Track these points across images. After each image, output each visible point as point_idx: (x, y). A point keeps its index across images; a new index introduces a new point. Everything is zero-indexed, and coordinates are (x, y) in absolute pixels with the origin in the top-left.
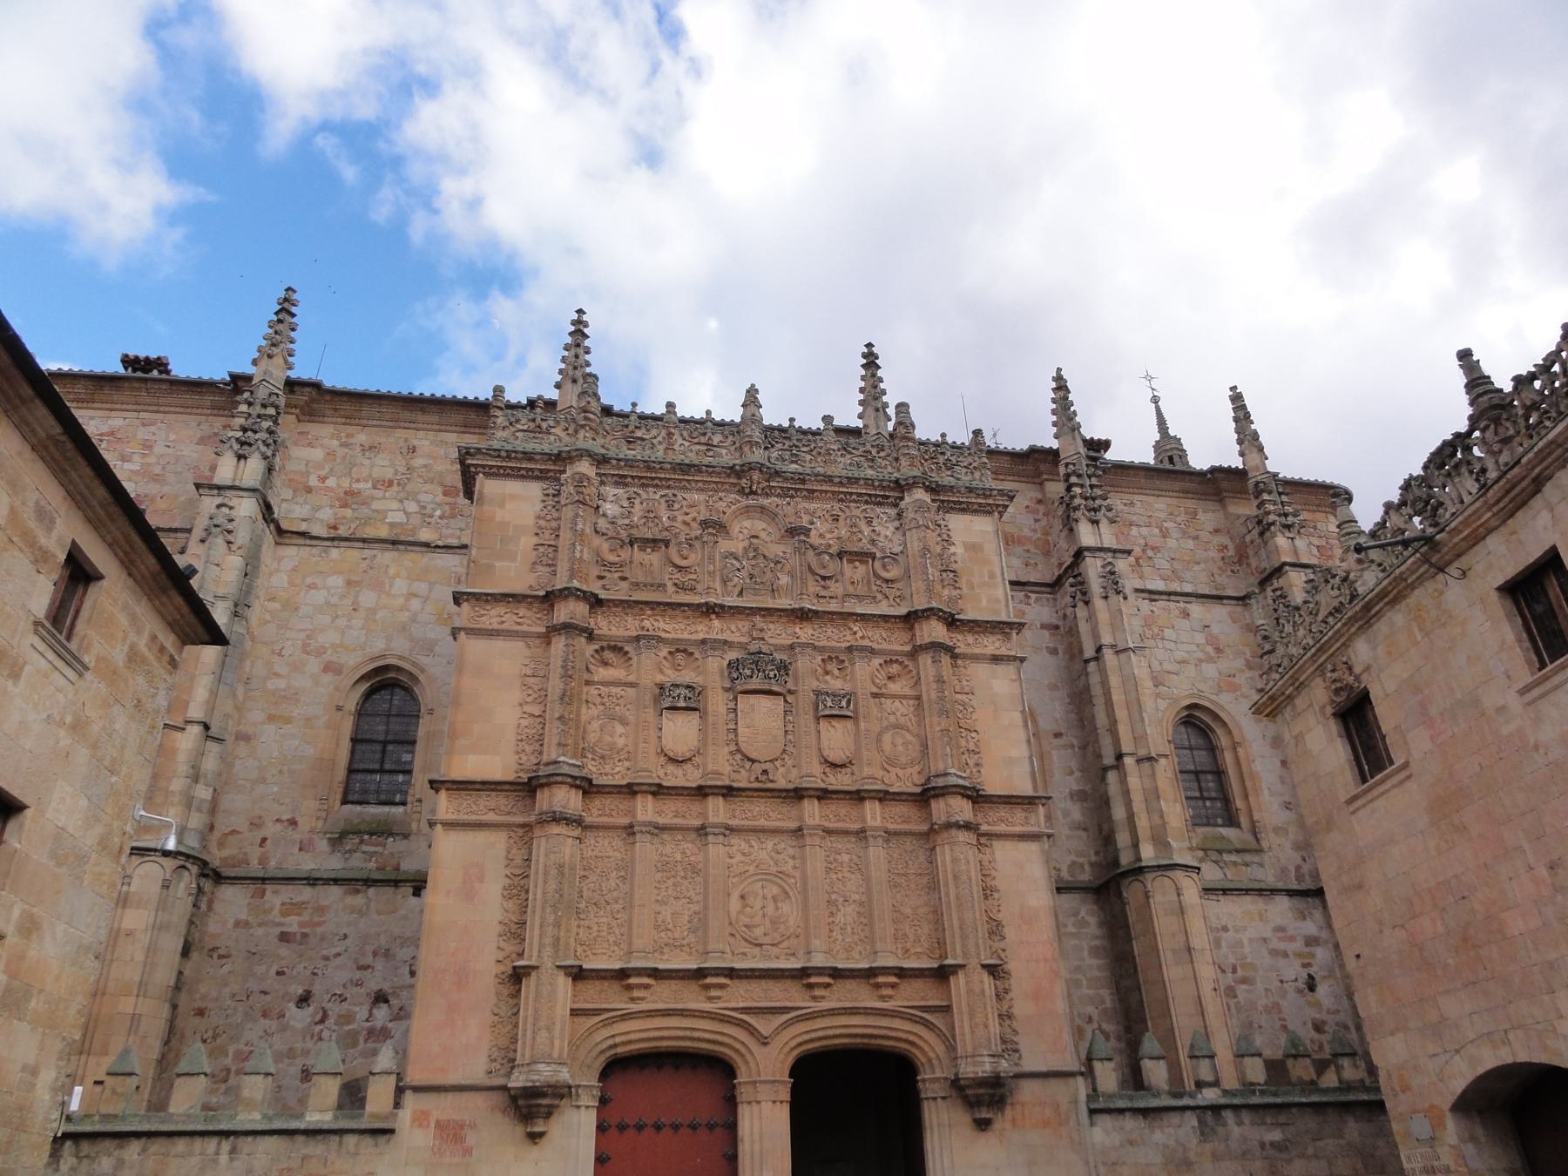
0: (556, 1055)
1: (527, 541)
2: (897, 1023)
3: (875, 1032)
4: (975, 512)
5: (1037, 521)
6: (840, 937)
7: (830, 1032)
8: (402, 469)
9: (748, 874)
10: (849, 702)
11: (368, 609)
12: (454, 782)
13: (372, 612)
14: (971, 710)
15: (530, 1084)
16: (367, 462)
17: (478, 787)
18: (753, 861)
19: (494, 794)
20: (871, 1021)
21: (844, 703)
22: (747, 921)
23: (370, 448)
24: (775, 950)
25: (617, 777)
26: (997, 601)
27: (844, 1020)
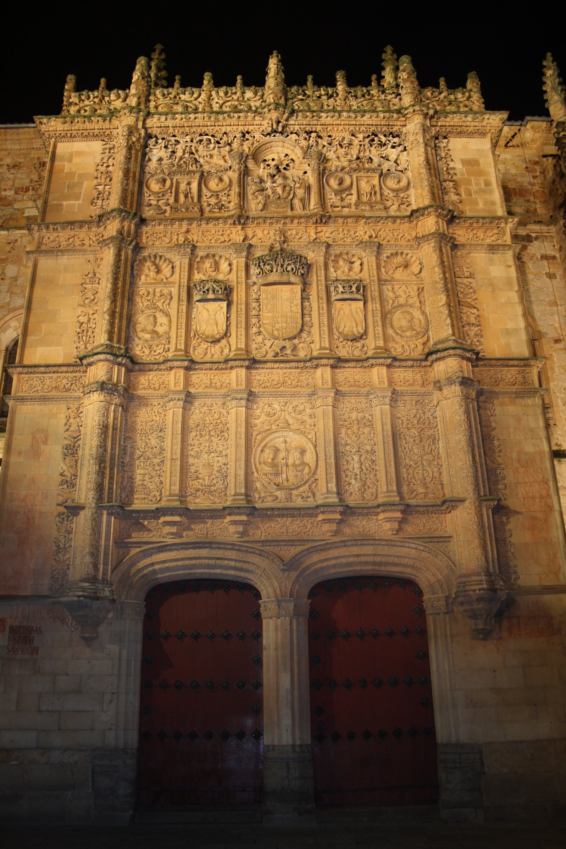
0: (100, 577)
1: (88, 185)
2: (404, 551)
3: (384, 559)
4: (470, 135)
5: (534, 177)
6: (353, 482)
7: (344, 561)
8: (35, 177)
9: (270, 432)
10: (358, 289)
11: (12, 278)
12: (24, 367)
13: (15, 279)
14: (471, 290)
15: (76, 599)
16: (11, 176)
17: (42, 369)
18: (275, 421)
19: (55, 375)
20: (380, 550)
21: (354, 289)
22: (267, 469)
23: (14, 167)
24: (295, 492)
25: (158, 357)
26: (493, 203)
27: (355, 550)
